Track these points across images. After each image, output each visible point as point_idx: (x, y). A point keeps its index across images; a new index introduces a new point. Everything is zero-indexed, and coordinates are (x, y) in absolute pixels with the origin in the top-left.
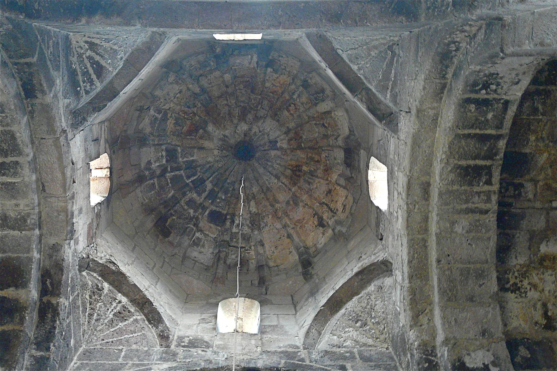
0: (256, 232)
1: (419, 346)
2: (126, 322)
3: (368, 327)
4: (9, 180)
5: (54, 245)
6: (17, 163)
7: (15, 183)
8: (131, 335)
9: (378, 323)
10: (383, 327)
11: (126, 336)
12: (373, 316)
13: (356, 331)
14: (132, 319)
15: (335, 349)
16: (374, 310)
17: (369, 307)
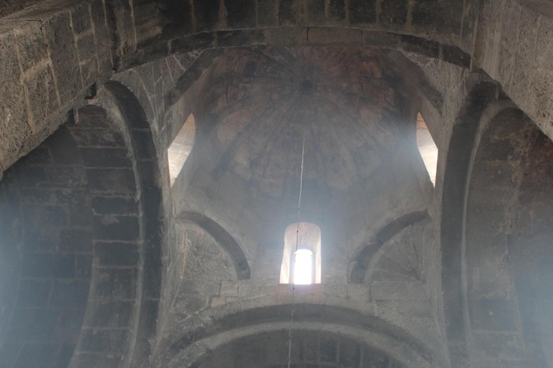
0: (240, 105)
1: (201, 328)
2: (180, 65)
3: (194, 258)
4: (327, 7)
5: (263, 35)
6: (343, 17)
7: (324, 11)
8: (170, 74)
9: (199, 266)
10: (197, 270)
11: (170, 70)
12: (203, 260)
13: (190, 249)
14: (183, 68)
15: (177, 241)
16: (208, 259)
17: (210, 255)
